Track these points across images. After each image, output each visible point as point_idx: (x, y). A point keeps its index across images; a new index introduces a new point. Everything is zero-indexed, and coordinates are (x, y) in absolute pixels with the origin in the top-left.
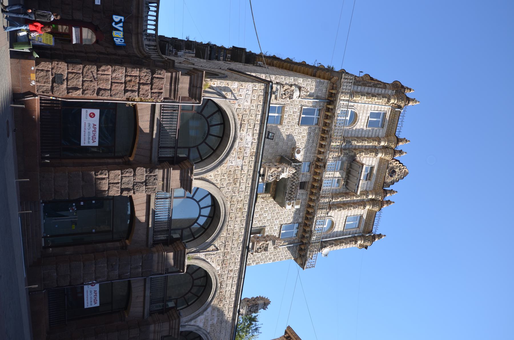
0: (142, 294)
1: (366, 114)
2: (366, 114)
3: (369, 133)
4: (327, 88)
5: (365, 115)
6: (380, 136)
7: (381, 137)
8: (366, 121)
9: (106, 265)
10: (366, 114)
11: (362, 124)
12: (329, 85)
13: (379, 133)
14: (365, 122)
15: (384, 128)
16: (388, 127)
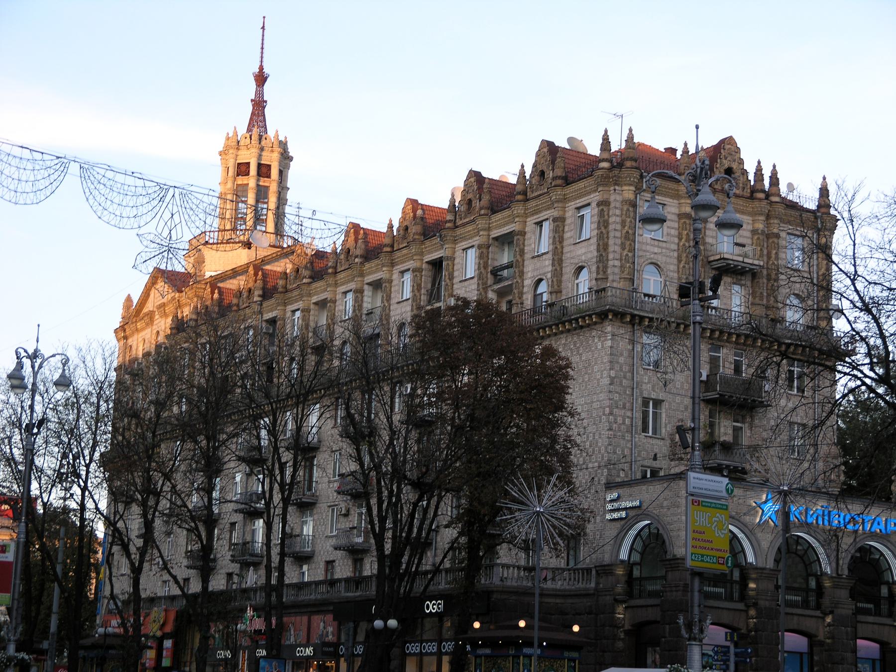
0: (871, 626)
1: (648, 244)
2: (648, 244)
3: (673, 236)
4: (619, 326)
5: (648, 248)
6: (677, 212)
7: (679, 207)
8: (656, 243)
9: (840, 666)
10: (647, 244)
11: (660, 250)
12: (615, 323)
13: (673, 214)
14: (658, 247)
15: (665, 203)
16: (665, 196)
